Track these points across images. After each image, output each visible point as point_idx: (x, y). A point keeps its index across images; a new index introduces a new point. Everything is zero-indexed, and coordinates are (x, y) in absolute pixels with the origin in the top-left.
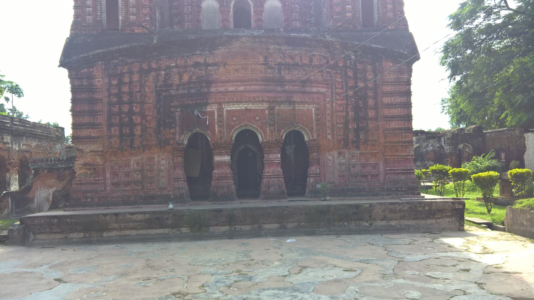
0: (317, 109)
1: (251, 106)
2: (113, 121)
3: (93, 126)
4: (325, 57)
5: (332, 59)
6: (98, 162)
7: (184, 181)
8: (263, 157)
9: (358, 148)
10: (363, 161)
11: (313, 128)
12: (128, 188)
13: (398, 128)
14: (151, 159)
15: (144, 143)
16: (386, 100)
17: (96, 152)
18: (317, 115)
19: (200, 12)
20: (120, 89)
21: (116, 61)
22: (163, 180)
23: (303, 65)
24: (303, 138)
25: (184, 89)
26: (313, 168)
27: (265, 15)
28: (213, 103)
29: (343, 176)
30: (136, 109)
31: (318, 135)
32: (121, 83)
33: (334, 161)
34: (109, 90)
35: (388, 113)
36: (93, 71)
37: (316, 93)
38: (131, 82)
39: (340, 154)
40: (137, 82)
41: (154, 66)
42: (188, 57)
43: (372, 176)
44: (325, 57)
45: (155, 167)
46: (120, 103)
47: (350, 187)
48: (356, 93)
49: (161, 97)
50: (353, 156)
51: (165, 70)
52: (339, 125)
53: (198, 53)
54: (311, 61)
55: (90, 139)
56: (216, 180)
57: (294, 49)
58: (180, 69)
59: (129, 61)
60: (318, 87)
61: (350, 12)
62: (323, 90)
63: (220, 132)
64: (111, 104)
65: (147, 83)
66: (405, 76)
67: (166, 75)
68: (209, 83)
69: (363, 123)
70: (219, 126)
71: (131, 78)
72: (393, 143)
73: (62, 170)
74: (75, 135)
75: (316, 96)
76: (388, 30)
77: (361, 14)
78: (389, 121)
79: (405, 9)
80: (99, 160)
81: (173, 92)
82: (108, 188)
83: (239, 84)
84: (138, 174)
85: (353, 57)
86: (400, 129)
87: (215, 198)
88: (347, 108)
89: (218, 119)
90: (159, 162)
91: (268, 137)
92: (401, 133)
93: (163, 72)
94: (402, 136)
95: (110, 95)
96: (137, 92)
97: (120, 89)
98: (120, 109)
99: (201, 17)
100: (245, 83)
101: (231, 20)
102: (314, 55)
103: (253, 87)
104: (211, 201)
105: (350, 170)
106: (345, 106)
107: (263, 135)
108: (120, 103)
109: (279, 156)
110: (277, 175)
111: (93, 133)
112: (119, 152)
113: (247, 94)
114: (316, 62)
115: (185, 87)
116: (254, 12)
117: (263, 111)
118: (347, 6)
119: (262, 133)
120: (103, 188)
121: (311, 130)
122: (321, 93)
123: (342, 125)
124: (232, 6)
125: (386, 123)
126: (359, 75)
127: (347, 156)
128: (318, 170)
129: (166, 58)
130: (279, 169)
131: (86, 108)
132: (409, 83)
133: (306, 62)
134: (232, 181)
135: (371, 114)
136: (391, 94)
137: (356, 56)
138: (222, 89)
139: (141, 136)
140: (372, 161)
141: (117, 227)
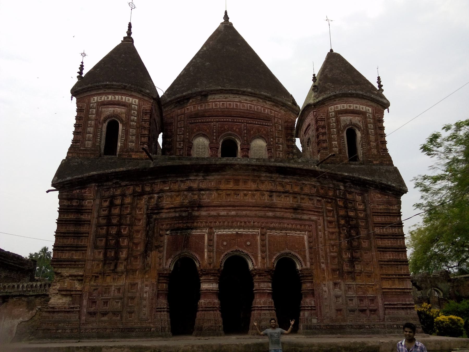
0: (309, 237)
1: (241, 231)
2: (99, 243)
3: (77, 248)
4: (315, 187)
5: (322, 189)
6: (76, 288)
7: (167, 311)
8: (253, 286)
9: (354, 279)
10: (360, 293)
11: (305, 256)
12: (105, 318)
13: (393, 259)
15: (129, 267)
16: (378, 231)
17: (75, 276)
18: (309, 242)
19: (191, 148)
20: (110, 211)
21: (110, 183)
22: (144, 309)
23: (295, 193)
25: (175, 212)
26: (308, 300)
27: (251, 154)
28: (204, 227)
29: (340, 310)
30: (125, 232)
31: (311, 264)
32: (112, 205)
34: (98, 212)
35: (382, 244)
36: (85, 193)
37: (307, 220)
38: (122, 205)
39: (335, 284)
40: (129, 204)
41: (148, 189)
42: (182, 181)
43: (371, 311)
44: (315, 187)
45: (138, 294)
46: (109, 224)
47: (348, 323)
48: (347, 222)
49: (152, 220)
50: (349, 288)
51: (158, 193)
52: (332, 254)
53: (191, 178)
54: (302, 189)
55: (72, 263)
56: (202, 310)
57: (285, 178)
58: (172, 193)
59: (123, 184)
60: (310, 214)
61: (336, 147)
62: (314, 218)
63: (209, 257)
64: (99, 226)
65: (138, 206)
66: (396, 207)
67: (159, 197)
68: (200, 207)
69: (357, 252)
70: (209, 251)
71: (123, 200)
72: (389, 275)
73: (33, 298)
74: (56, 257)
75: (307, 223)
76: (374, 165)
78: (383, 251)
79: (388, 146)
80: (78, 286)
81: (164, 216)
82: (83, 318)
84: (118, 302)
85: (342, 188)
86: (396, 261)
87: (201, 332)
88: (340, 237)
89: (208, 243)
90: (142, 288)
91: (260, 264)
92: (397, 265)
93: (156, 195)
94: (397, 268)
95: (99, 217)
96: (128, 214)
97: (110, 211)
98: (108, 231)
99: (192, 152)
100: (237, 208)
102: (304, 184)
103: (244, 213)
104: (196, 336)
105: (347, 304)
106: (337, 234)
107: (254, 261)
108: (109, 224)
109: (270, 285)
110: (269, 307)
111: (76, 256)
112: (100, 276)
113: (237, 219)
114: (306, 190)
115: (177, 210)
116: (241, 149)
117: (254, 236)
118: (333, 142)
119: (253, 259)
120: (78, 317)
121: (304, 258)
122: (313, 221)
123: (335, 254)
124: (221, 144)
125: (381, 253)
126: (350, 205)
127: (343, 288)
128: (313, 302)
129: (161, 182)
130: (271, 300)
131: (72, 229)
132: (399, 215)
133: (296, 190)
135: (365, 244)
136: (382, 225)
137: (345, 187)
138: (213, 213)
139: (126, 259)
140: (370, 294)
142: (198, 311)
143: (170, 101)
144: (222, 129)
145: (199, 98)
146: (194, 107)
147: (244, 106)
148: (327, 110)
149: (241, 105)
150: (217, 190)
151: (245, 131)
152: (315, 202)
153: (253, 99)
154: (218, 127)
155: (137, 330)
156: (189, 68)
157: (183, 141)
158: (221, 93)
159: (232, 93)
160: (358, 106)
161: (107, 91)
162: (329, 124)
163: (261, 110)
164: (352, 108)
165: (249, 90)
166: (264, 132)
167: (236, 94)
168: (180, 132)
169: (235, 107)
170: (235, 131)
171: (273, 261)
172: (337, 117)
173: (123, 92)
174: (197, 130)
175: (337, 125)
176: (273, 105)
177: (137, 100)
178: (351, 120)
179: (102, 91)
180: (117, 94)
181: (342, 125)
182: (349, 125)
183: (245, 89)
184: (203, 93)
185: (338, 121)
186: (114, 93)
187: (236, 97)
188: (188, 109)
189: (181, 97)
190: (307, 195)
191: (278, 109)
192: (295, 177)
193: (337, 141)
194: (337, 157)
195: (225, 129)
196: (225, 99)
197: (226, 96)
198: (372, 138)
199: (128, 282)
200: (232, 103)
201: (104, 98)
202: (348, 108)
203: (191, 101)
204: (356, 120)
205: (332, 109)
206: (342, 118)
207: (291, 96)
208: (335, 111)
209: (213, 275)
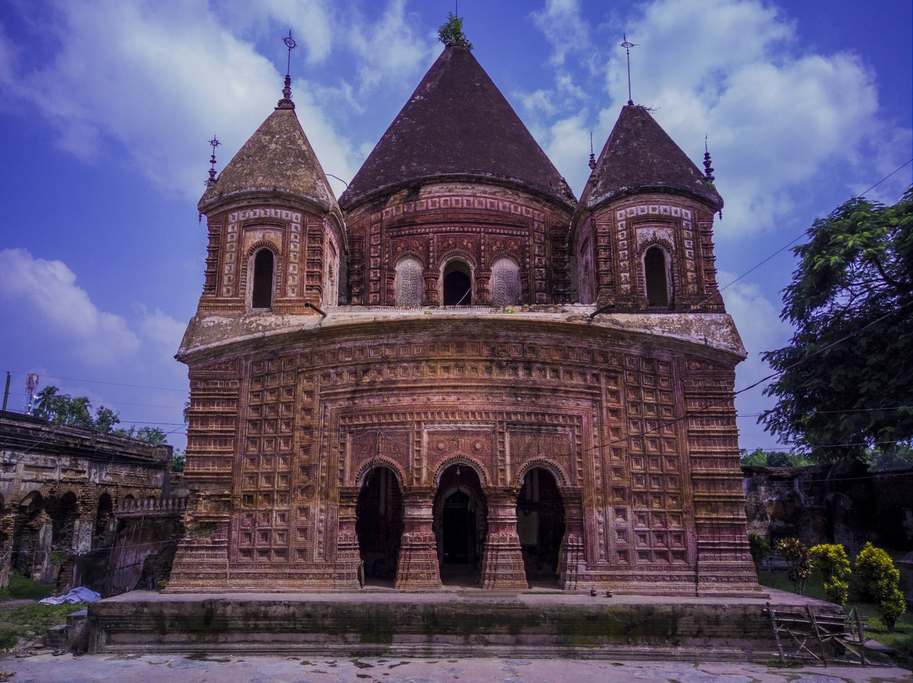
4: (588, 353)
8: (486, 512)
12: (264, 559)
14: (304, 510)
24: (554, 482)
33: (606, 525)
54: (566, 357)
56: (407, 550)
61: (627, 283)
77: (645, 285)
83: (450, 390)
99: (395, 286)
101: (441, 289)
102: (569, 347)
109: (514, 511)
110: (510, 546)
116: (476, 278)
118: (622, 275)
124: (441, 269)
130: (514, 534)
134: (435, 552)
141: (241, 626)
142: (402, 549)
143: (357, 201)
144: (445, 245)
145: (405, 192)
146: (397, 208)
147: (480, 203)
148: (614, 218)
149: (476, 201)
150: (427, 361)
151: (483, 247)
152: (588, 377)
153: (497, 189)
154: (438, 241)
155: (311, 576)
156: (391, 137)
157: (380, 268)
158: (442, 182)
159: (460, 182)
160: (668, 208)
161: (253, 202)
162: (616, 244)
163: (510, 209)
164: (657, 212)
165: (489, 175)
166: (515, 247)
167: (467, 182)
168: (375, 252)
169: (465, 205)
170: (466, 248)
171: (518, 473)
172: (630, 228)
173: (277, 202)
174: (403, 249)
175: (630, 245)
176: (531, 199)
177: (299, 215)
178: (654, 234)
179: (245, 203)
180: (269, 206)
181: (640, 242)
182: (651, 243)
183: (483, 174)
184: (412, 185)
185: (631, 237)
186: (262, 205)
187: (467, 188)
188: (387, 212)
189: (375, 193)
190: (577, 366)
191: (539, 206)
192: (556, 336)
193: (629, 271)
194: (629, 300)
195: (449, 245)
196: (449, 191)
197: (451, 186)
198: (689, 265)
199: (295, 505)
200: (460, 198)
201: (250, 214)
202: (651, 212)
203: (392, 198)
204: (664, 233)
205: (621, 214)
206: (639, 231)
207: (564, 181)
208: (627, 219)
209: (424, 495)
